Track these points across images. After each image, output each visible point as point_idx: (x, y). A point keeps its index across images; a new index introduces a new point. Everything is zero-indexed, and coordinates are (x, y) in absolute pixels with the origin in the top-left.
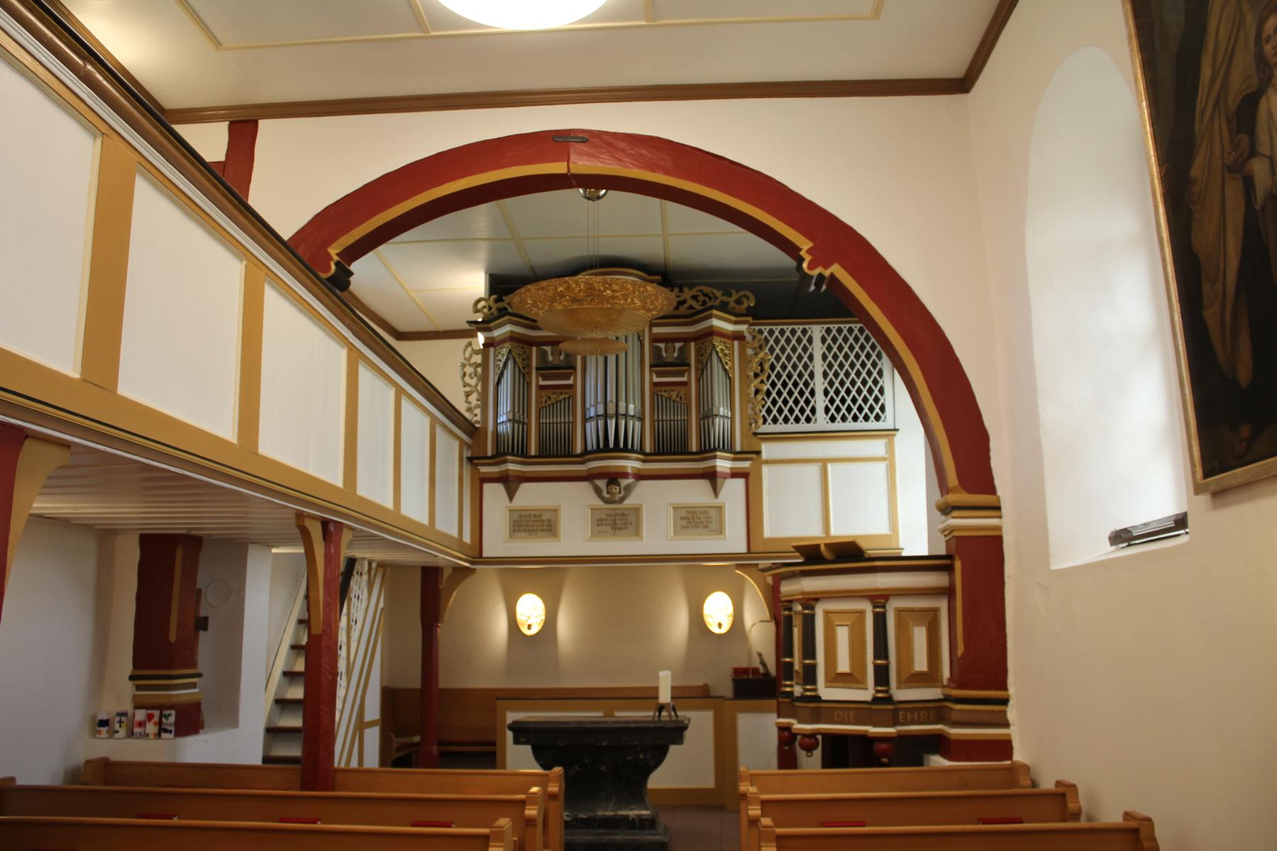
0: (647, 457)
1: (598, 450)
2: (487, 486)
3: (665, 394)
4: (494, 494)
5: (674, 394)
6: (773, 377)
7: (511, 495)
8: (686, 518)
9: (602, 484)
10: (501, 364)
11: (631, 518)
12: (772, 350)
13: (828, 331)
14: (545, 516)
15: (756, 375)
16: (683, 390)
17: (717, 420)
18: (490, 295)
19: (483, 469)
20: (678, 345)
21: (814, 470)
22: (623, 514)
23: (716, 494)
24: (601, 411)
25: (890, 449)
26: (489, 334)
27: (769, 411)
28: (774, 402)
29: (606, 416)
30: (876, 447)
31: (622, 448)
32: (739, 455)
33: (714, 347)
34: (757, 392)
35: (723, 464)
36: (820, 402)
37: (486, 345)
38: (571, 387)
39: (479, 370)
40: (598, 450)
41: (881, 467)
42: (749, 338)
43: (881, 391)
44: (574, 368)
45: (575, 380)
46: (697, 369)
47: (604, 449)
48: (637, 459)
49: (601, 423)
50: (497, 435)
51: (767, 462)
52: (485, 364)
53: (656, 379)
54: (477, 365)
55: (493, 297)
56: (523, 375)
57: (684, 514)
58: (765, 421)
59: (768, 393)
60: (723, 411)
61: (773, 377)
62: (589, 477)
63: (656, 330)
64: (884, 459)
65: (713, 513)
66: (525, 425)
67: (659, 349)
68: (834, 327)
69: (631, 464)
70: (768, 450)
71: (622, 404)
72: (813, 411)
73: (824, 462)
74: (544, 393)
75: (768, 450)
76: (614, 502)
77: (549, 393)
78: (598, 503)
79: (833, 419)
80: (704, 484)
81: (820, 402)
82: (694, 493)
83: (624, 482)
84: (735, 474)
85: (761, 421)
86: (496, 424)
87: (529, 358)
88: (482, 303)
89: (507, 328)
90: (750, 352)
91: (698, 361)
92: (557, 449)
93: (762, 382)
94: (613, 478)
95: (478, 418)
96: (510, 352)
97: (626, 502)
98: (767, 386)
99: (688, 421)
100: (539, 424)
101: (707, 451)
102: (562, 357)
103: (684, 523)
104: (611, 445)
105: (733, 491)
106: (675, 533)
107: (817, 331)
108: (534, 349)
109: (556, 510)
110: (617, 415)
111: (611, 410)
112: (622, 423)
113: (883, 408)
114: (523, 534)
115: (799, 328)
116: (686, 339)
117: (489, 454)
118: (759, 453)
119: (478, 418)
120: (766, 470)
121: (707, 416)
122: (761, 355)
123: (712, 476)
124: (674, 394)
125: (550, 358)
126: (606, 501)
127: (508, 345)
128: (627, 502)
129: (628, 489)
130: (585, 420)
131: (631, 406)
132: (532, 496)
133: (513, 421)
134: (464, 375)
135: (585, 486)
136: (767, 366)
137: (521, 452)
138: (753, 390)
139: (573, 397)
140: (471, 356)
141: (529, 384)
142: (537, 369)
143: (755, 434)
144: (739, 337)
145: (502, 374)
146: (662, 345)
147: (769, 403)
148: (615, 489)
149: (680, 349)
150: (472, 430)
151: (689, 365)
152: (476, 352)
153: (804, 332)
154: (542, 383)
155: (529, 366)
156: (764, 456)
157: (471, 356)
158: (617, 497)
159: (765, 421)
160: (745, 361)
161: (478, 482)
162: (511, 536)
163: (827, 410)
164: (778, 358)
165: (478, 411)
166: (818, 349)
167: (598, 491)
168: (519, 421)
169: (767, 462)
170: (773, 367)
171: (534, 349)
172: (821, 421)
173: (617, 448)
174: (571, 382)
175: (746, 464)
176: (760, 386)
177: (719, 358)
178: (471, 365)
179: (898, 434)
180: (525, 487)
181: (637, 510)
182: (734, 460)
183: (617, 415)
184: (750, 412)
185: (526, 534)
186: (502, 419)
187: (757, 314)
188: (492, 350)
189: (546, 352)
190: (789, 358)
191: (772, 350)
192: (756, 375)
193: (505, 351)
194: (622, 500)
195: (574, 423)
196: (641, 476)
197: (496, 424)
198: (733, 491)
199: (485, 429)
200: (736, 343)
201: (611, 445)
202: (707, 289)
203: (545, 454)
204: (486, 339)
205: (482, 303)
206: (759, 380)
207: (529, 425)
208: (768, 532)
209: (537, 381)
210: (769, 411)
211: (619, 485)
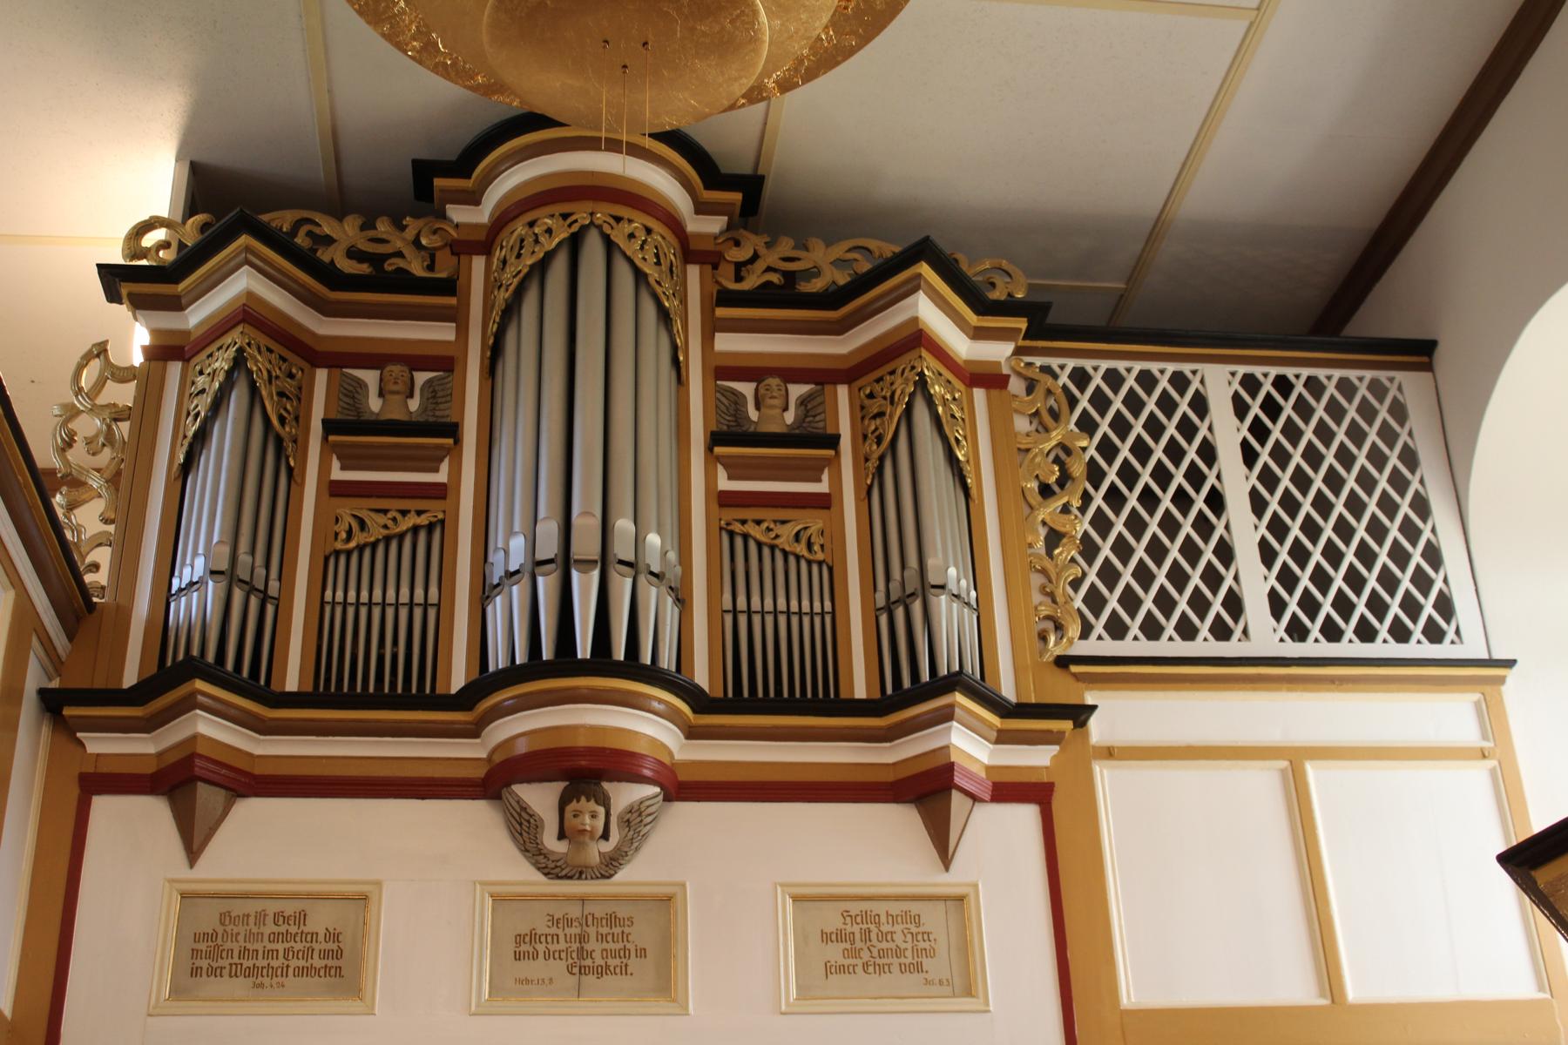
0: (706, 709)
1: (535, 668)
2: (103, 806)
3: (756, 532)
4: (131, 833)
5: (787, 532)
6: (1098, 500)
7: (193, 853)
8: (840, 936)
9: (540, 798)
10: (203, 404)
11: (642, 934)
12: (1086, 424)
13: (1251, 383)
14: (321, 920)
15: (1046, 491)
16: (815, 522)
17: (942, 602)
18: (191, 209)
19: (99, 745)
20: (797, 391)
21: (1263, 781)
22: (612, 919)
23: (945, 853)
24: (549, 546)
25: (1492, 718)
26: (169, 321)
27: (1095, 601)
28: (1109, 575)
29: (565, 562)
30: (1448, 715)
31: (618, 664)
32: (1019, 716)
33: (922, 383)
34: (1054, 538)
35: (970, 745)
36: (1254, 582)
37: (164, 351)
38: (439, 492)
39: (124, 428)
40: (535, 668)
41: (1477, 776)
42: (1016, 386)
43: (1433, 555)
44: (453, 431)
45: (456, 472)
46: (861, 460)
47: (556, 664)
48: (672, 715)
49: (547, 586)
50: (161, 630)
51: (1109, 753)
52: (144, 413)
53: (724, 484)
54: (119, 415)
55: (199, 218)
56: (278, 450)
57: (831, 918)
58: (1086, 631)
59: (1089, 550)
60: (955, 575)
61: (1098, 500)
62: (492, 783)
63: (726, 343)
64: (1484, 755)
65: (934, 919)
66: (271, 603)
67: (738, 398)
68: (1267, 374)
69: (651, 727)
70: (1118, 715)
71: (623, 525)
72: (1234, 604)
73: (1293, 762)
74: (346, 509)
75: (1118, 715)
76: (580, 874)
77: (362, 507)
78: (521, 874)
79: (1297, 631)
80: (898, 823)
81: (1254, 582)
82: (871, 848)
83: (625, 795)
84: (1007, 790)
85: (1074, 630)
86: (165, 596)
87: (302, 396)
88: (160, 234)
89: (241, 283)
90: (1022, 424)
91: (861, 437)
92: (379, 681)
93: (1066, 509)
94: (586, 770)
95: (101, 578)
96: (239, 361)
97: (620, 876)
98: (1084, 525)
99: (836, 616)
100: (319, 606)
101: (915, 690)
102: (414, 404)
103: (834, 953)
104: (584, 649)
105: (1000, 841)
106: (804, 992)
107: (1218, 381)
108: (321, 375)
109: (364, 898)
110: (605, 561)
111: (586, 543)
112: (622, 588)
113: (1445, 606)
114: (226, 985)
115: (1163, 370)
116: (823, 376)
117: (130, 679)
118: (1080, 714)
119: (101, 578)
120: (1105, 776)
121: (904, 597)
122: (1056, 436)
123: (929, 791)
124: (787, 532)
125: (375, 404)
126: (552, 869)
127: (236, 337)
128: (635, 874)
129: (636, 820)
130: (484, 593)
131: (653, 539)
132: (269, 844)
133: (227, 575)
134: (69, 443)
135: (477, 815)
136: (1078, 469)
137: (251, 683)
138: (1043, 532)
139: (441, 527)
140: (100, 385)
141: (295, 477)
142: (330, 426)
143: (1063, 662)
144: (991, 379)
145: (202, 436)
146: (746, 389)
147: (1092, 577)
148: (589, 815)
149: (803, 402)
150: (77, 606)
151: (833, 441)
152: (124, 375)
153: (1180, 381)
154: (337, 474)
155: (301, 419)
156: (1098, 729)
157: (100, 385)
158: (596, 851)
159: (1086, 631)
160: (1010, 452)
161: (75, 792)
162: (177, 992)
163: (1277, 606)
164: (1107, 449)
165: (103, 556)
166: (1227, 432)
167: (523, 828)
168: (251, 585)
169: (1109, 753)
170: (1095, 475)
171: (321, 375)
172: (1263, 633)
173: (602, 661)
174: (441, 477)
175: (1037, 758)
176: (1061, 524)
177: (937, 422)
178: (94, 410)
179: (1511, 675)
180: (253, 817)
181: (665, 903)
182: (1003, 738)
183: (605, 561)
184: (1037, 598)
185: (240, 985)
186: (192, 568)
187: (1042, 323)
188: (175, 369)
189: (361, 385)
190: (1141, 450)
191: (1086, 424)
192: (1046, 491)
193: (222, 363)
194: (611, 864)
195: (443, 608)
196: (684, 787)
197: (165, 596)
198: (1000, 841)
199: (123, 614)
200: (979, 394)
201: (584, 649)
202: (873, 244)
203: (338, 693)
204: (155, 333)
205: (160, 234)
206: (1058, 504)
207: (282, 605)
208: (1134, 990)
209: (324, 468)
210: (1095, 601)
211: (605, 801)
